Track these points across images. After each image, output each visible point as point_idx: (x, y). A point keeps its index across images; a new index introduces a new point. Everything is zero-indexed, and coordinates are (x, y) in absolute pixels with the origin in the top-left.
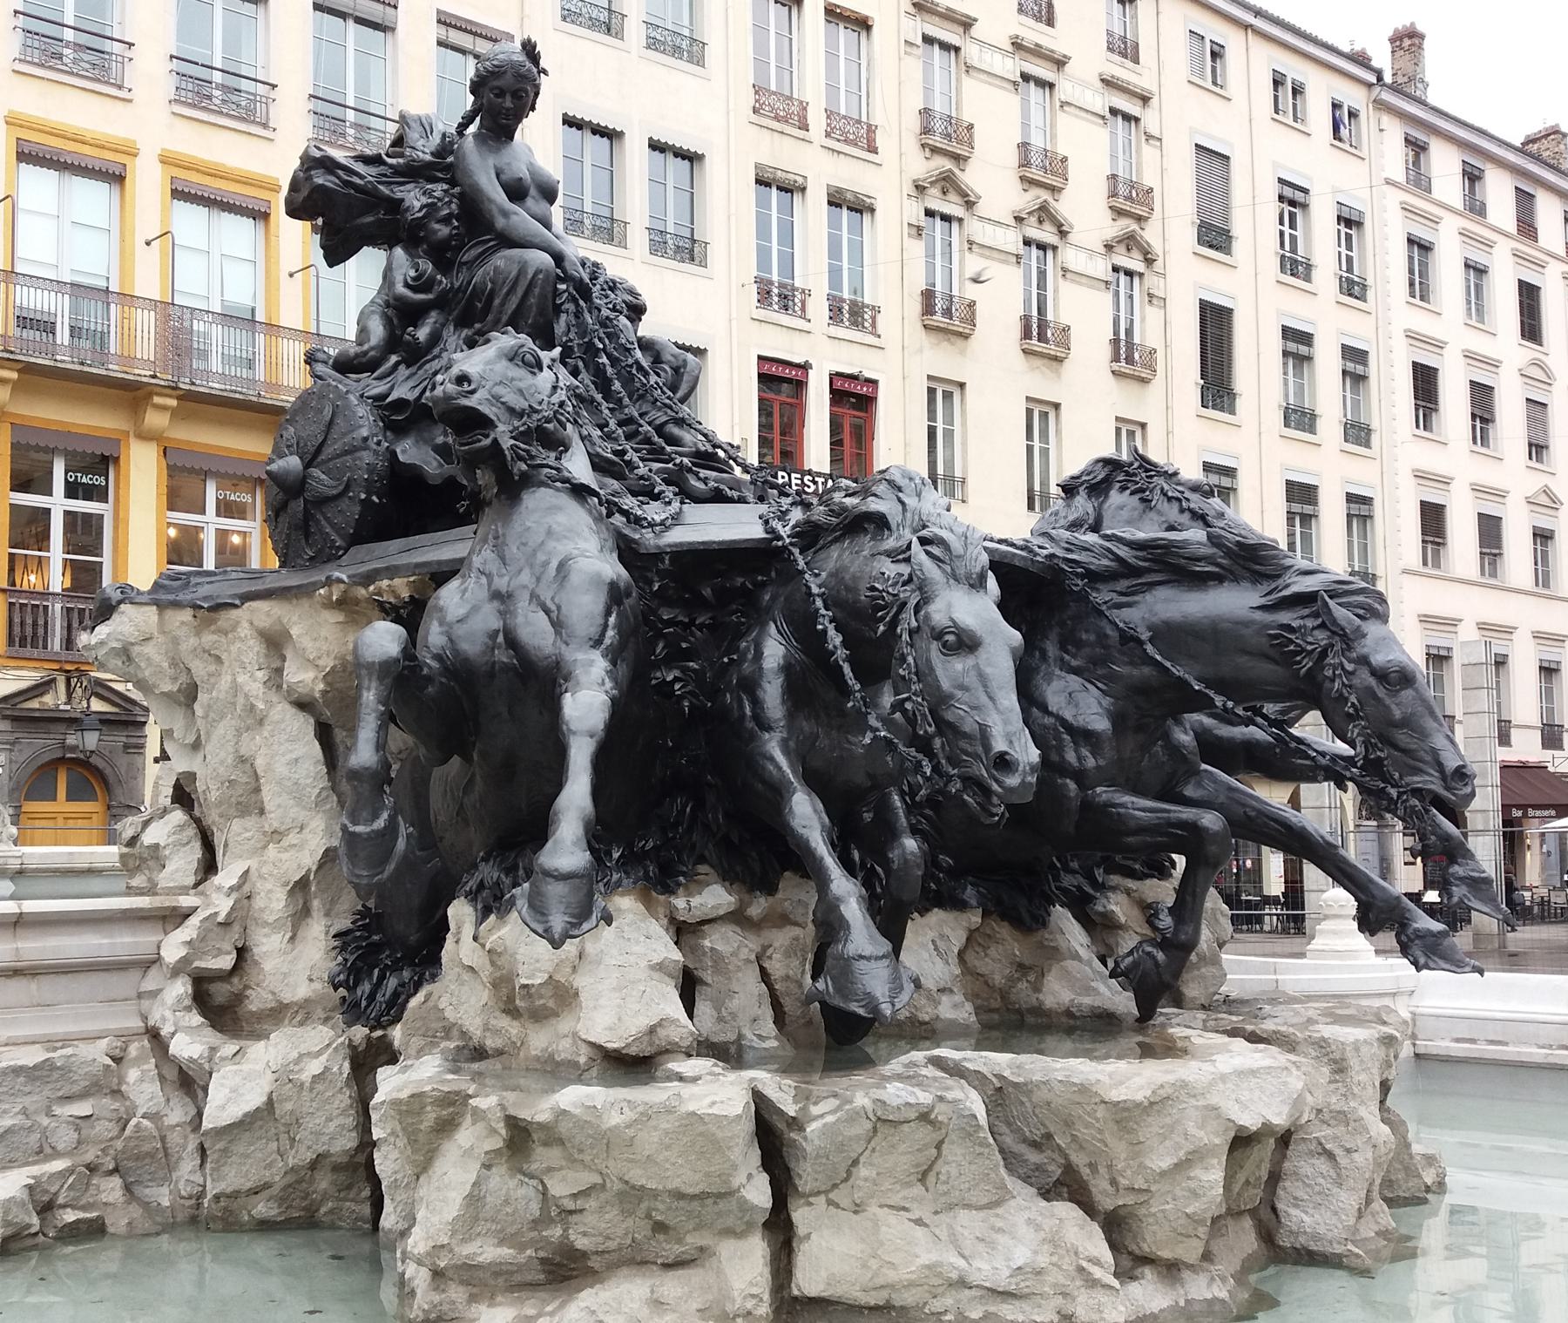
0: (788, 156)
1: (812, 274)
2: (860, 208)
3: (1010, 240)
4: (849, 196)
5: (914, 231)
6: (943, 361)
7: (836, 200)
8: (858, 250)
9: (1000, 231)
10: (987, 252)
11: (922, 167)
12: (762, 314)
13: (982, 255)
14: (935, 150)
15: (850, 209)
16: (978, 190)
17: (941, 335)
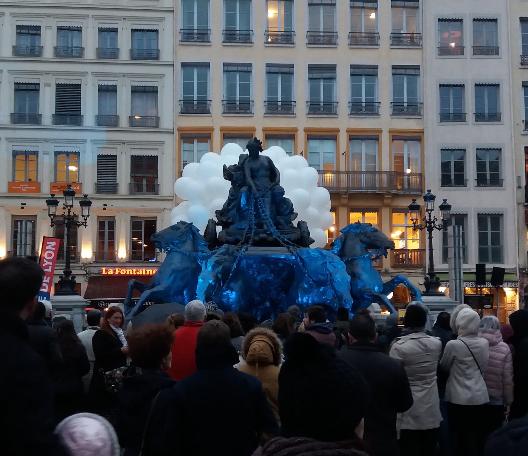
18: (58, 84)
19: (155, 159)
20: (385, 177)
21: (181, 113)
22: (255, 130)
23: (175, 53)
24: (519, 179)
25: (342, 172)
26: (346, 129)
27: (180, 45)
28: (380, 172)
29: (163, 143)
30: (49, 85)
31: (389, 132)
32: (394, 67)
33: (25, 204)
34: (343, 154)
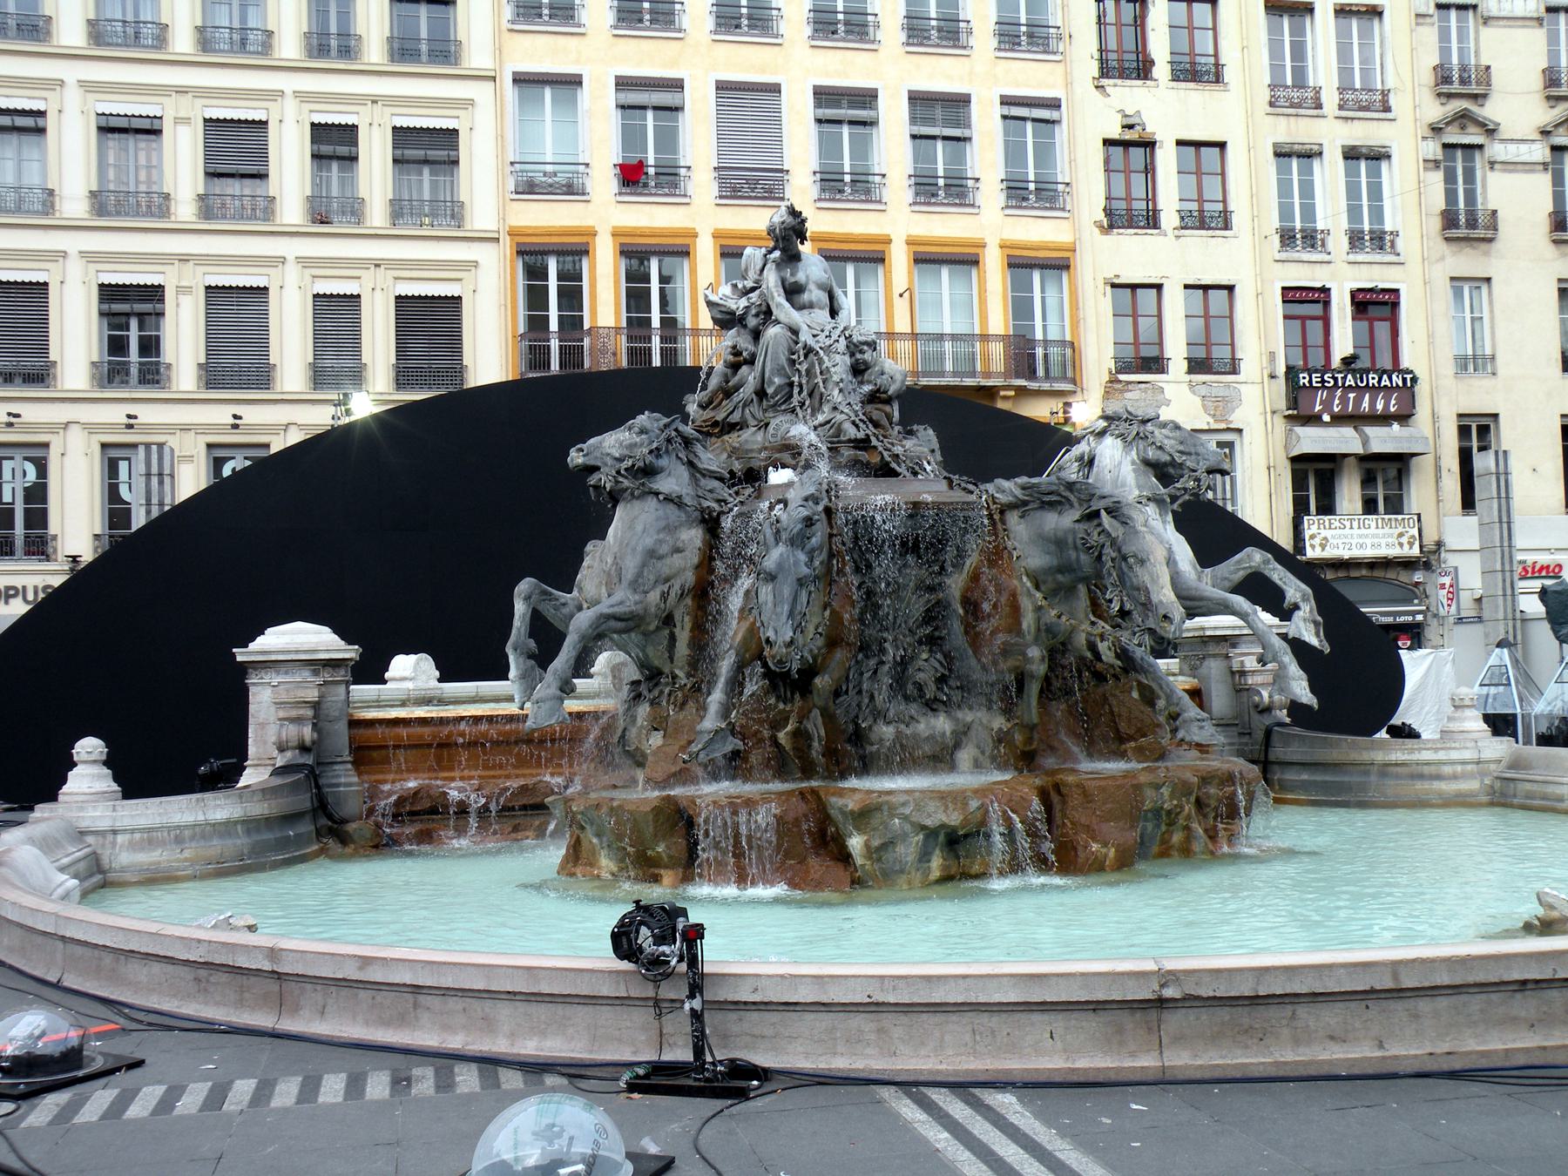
0: (1300, 131)
1: (1331, 215)
2: (1377, 156)
3: (1540, 152)
4: (1364, 150)
5: (1431, 165)
6: (1467, 262)
7: (1352, 154)
8: (1376, 192)
9: (1524, 148)
10: (1511, 167)
11: (1436, 111)
12: (1284, 256)
13: (1505, 171)
14: (1450, 96)
15: (1367, 159)
16: (1498, 120)
17: (1463, 244)
18: (211, 120)
19: (453, 303)
20: (997, 349)
21: (517, 193)
22: (696, 236)
23: (499, 51)
24: (1272, 356)
25: (902, 336)
26: (905, 238)
27: (511, 30)
28: (985, 338)
29: (476, 264)
30: (186, 121)
31: (1001, 247)
32: (1006, 101)
33: (136, 417)
34: (901, 295)
